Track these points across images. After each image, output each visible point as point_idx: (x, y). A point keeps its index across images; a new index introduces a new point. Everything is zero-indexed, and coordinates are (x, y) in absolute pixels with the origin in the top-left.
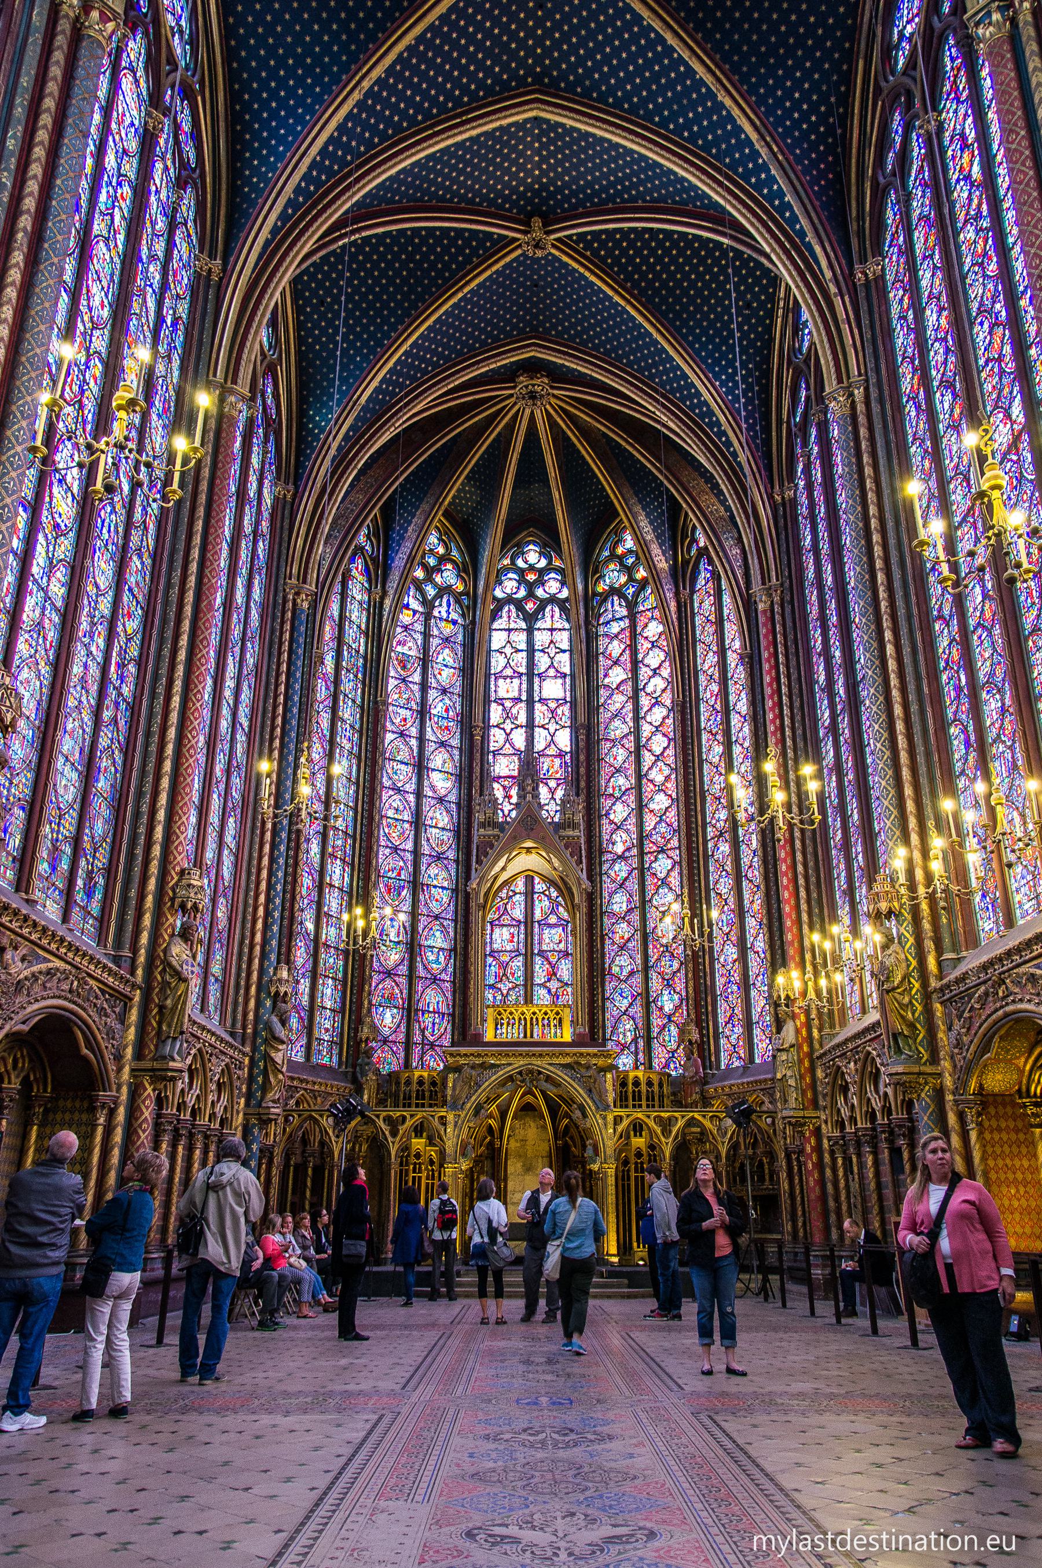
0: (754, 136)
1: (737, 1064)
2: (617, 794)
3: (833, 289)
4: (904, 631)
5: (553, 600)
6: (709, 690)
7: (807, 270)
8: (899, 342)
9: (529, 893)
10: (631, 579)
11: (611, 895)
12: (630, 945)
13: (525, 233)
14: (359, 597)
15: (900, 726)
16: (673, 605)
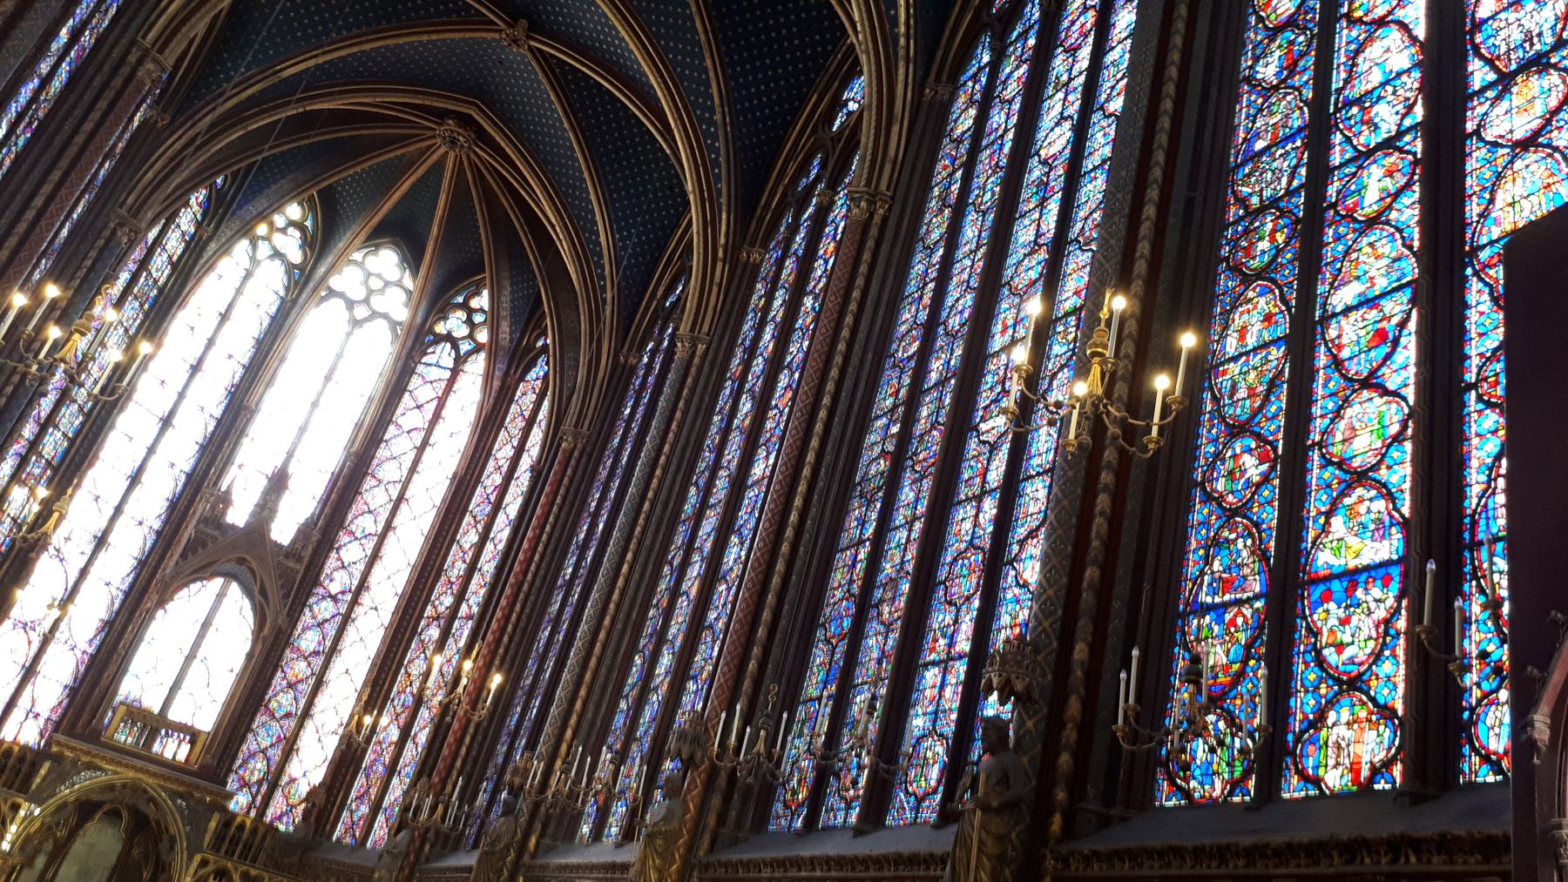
0: (717, 101)
1: (348, 840)
2: (358, 535)
4: (641, 559)
5: (385, 316)
6: (492, 479)
7: (710, 224)
8: (746, 328)
9: (221, 595)
10: (471, 336)
11: (304, 630)
12: (300, 687)
13: (511, 26)
14: (184, 228)
15: (602, 636)
16: (497, 383)
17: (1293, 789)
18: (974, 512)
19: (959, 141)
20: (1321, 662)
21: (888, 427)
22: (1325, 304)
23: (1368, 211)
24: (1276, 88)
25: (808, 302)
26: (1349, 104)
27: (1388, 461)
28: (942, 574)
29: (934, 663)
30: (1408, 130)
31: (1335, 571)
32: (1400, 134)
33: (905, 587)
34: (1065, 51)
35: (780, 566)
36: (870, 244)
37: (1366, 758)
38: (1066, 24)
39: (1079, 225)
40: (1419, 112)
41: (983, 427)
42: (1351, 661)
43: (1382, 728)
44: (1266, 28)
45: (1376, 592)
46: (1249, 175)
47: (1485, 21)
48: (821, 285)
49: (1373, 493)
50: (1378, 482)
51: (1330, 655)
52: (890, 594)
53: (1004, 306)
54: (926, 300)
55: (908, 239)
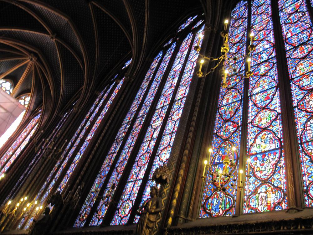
0: (96, 57)
3: (90, 91)
7: (89, 84)
16: (27, 118)
17: (246, 210)
18: (148, 144)
19: (152, 69)
20: (255, 176)
21: (126, 126)
23: (261, 74)
24: (235, 53)
25: (109, 102)
27: (273, 125)
28: (137, 160)
29: (132, 181)
31: (258, 152)
32: (269, 59)
33: (126, 163)
35: (91, 157)
36: (129, 86)
38: (181, 47)
39: (183, 82)
41: (153, 125)
42: (265, 175)
43: (277, 193)
45: (272, 157)
47: (288, 38)
48: (113, 98)
49: (269, 133)
50: (270, 130)
51: (258, 174)
52: (121, 165)
53: (162, 99)
54: (141, 99)
55: (138, 87)
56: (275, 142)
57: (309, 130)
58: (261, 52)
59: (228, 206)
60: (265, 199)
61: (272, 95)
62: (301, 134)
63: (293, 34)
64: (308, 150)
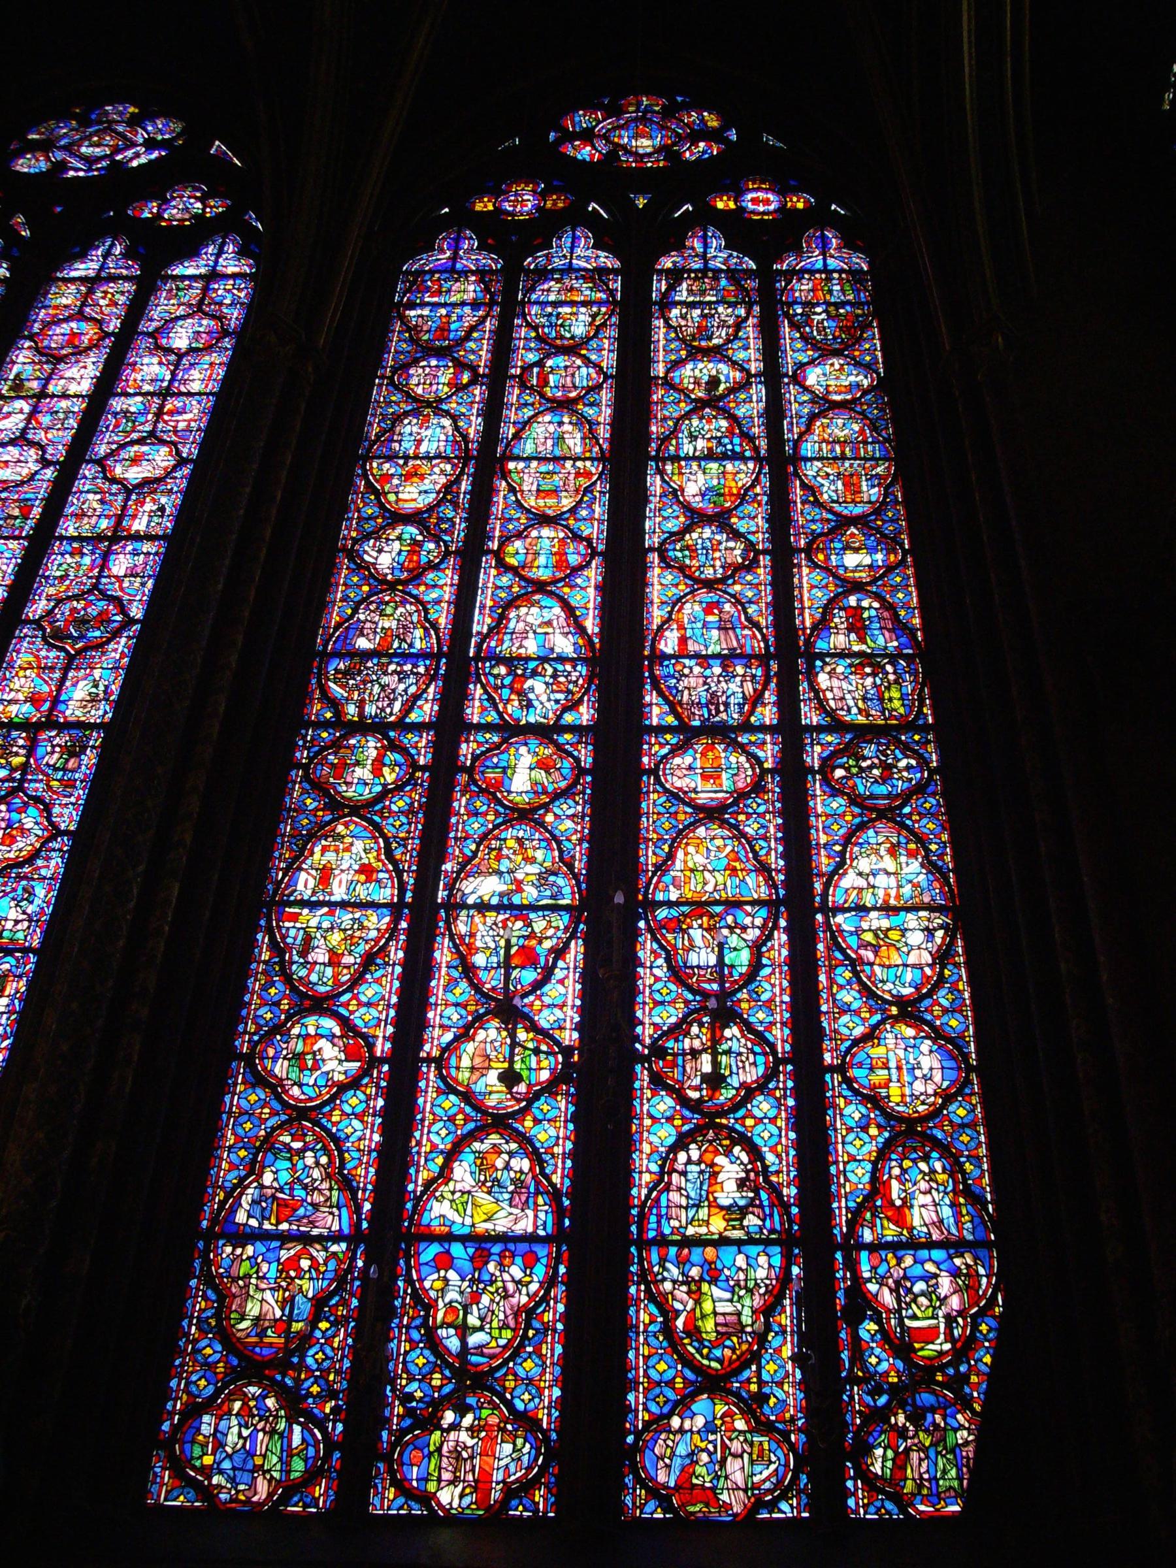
17: (386, 1501)
20: (433, 1343)
22: (450, 887)
24: (392, 586)
26: (500, 660)
30: (571, 729)
31: (457, 1230)
34: (38, 351)
37: (498, 1476)
40: (585, 715)
44: (381, 506)
46: (347, 673)
47: (665, 657)
49: (514, 1146)
50: (523, 1135)
56: (535, 1203)
57: (679, 1189)
58: (528, 659)
59: (298, 1465)
60: (472, 1457)
61: (551, 950)
62: (648, 1196)
63: (692, 647)
64: (664, 1279)
